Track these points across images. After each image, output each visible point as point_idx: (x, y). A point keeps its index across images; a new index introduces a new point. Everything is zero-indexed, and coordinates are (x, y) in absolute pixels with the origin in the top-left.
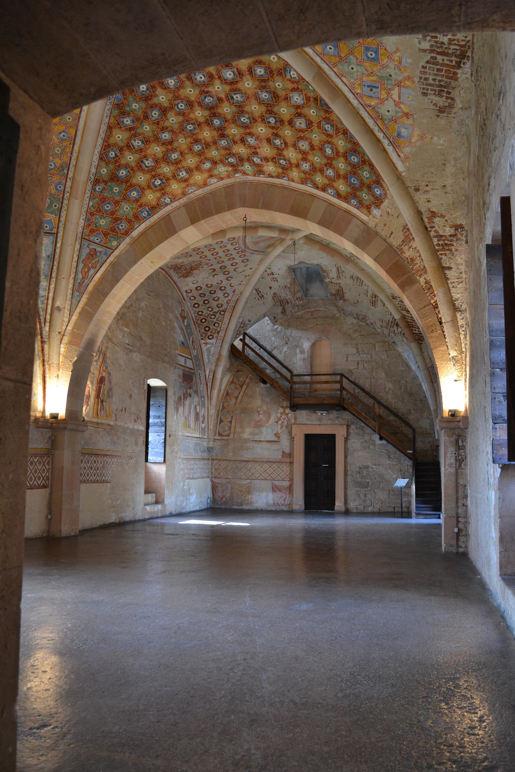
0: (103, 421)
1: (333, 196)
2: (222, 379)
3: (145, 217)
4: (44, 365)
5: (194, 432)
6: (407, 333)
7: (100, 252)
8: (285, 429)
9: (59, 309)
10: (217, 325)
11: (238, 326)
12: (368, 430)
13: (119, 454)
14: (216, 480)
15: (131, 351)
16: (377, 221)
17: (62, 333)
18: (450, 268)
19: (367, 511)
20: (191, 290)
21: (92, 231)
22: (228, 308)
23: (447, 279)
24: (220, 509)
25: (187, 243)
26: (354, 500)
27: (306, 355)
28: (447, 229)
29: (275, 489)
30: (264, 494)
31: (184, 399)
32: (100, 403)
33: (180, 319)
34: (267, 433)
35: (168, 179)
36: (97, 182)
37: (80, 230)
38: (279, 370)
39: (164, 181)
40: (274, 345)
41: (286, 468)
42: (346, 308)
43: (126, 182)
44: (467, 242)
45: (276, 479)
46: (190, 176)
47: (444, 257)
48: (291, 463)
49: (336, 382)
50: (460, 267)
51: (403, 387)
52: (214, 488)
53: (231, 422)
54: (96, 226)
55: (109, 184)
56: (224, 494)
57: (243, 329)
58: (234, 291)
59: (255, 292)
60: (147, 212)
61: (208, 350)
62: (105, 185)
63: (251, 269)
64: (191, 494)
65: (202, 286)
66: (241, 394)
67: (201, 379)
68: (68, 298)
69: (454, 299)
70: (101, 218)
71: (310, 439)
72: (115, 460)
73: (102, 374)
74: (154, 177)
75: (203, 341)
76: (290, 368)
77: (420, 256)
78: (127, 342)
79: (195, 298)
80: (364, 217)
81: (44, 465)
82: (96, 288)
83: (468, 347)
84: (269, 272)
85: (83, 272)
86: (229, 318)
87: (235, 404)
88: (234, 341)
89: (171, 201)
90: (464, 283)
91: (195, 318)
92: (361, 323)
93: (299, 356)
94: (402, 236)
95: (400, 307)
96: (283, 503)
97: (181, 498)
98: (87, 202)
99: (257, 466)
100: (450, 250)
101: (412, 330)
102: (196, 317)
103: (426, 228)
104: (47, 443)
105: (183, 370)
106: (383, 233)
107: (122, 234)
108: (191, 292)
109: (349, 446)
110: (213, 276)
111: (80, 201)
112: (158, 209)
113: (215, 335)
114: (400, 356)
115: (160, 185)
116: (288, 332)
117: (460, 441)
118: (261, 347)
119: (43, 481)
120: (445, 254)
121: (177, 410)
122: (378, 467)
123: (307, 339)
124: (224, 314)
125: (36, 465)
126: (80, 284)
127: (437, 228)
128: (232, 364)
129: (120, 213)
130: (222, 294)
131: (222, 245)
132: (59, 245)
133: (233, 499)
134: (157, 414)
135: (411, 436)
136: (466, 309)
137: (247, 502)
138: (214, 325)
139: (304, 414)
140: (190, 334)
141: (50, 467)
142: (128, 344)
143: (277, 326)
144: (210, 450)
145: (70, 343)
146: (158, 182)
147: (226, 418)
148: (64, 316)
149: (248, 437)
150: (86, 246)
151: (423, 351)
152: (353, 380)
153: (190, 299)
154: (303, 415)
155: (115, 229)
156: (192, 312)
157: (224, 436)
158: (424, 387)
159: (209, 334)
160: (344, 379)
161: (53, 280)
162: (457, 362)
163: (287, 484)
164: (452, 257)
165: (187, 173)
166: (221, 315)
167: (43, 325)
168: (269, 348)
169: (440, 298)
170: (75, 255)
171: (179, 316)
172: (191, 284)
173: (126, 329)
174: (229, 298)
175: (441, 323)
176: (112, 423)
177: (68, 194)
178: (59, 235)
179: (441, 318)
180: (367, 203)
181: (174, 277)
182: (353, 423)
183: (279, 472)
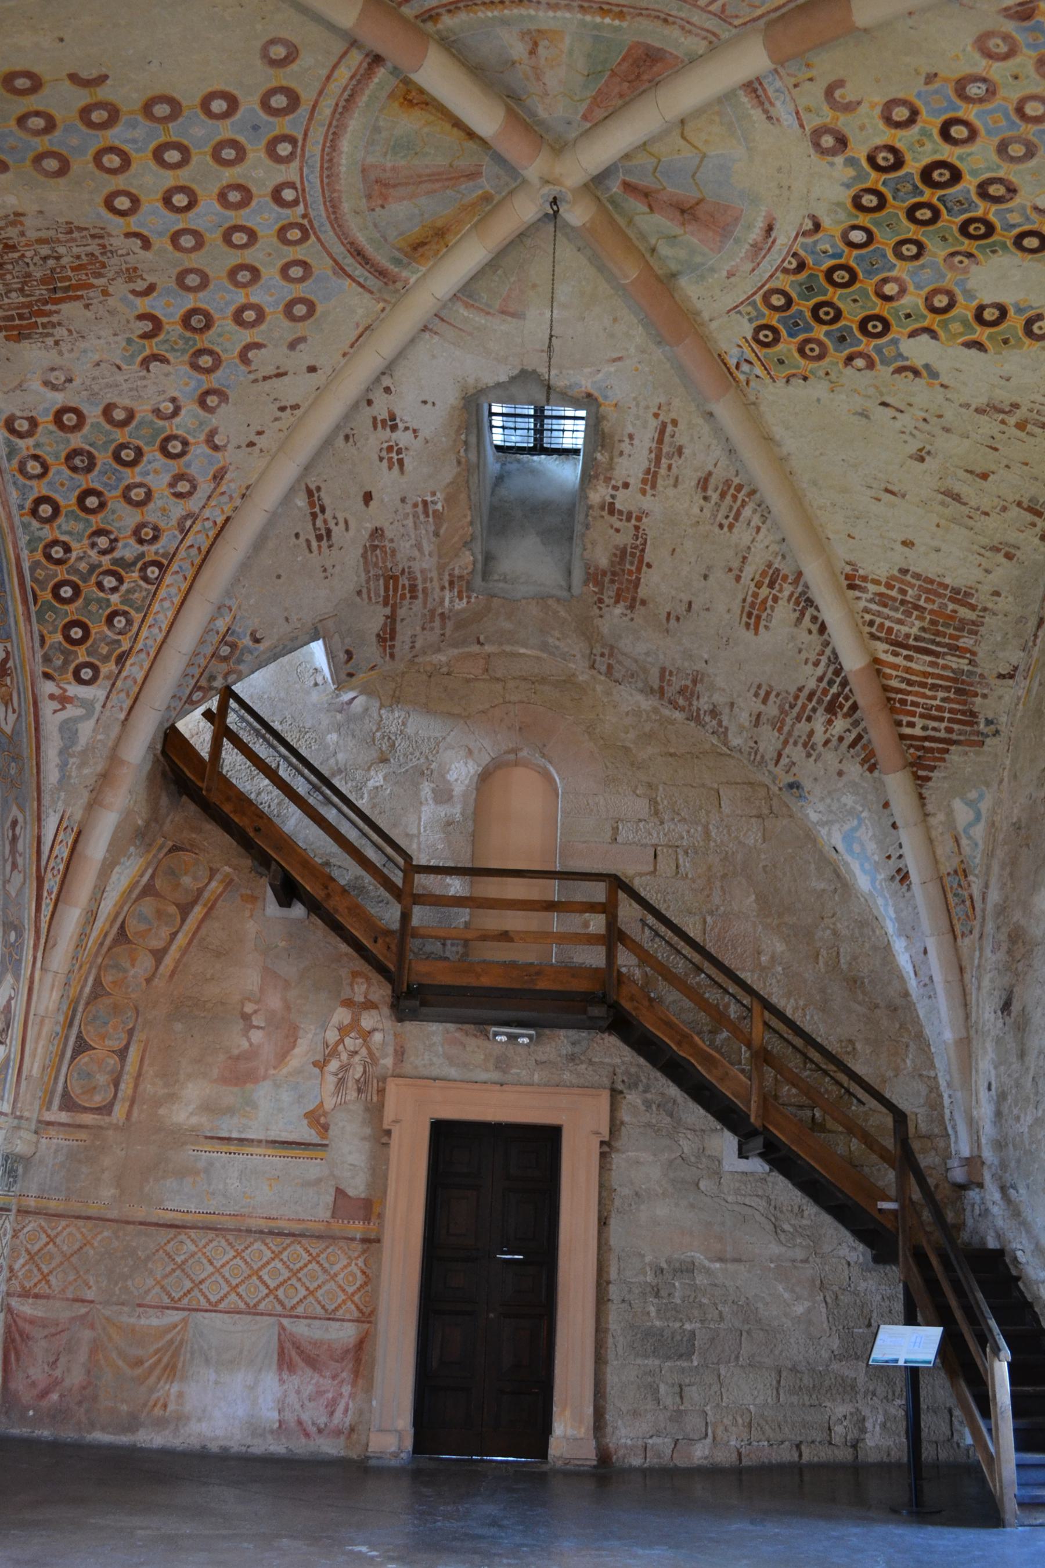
2: (108, 871)
6: (880, 734)
8: (352, 1095)
10: (120, 622)
11: (209, 650)
14: (26, 1308)
20: (33, 422)
22: (182, 553)
26: (635, 1413)
27: (456, 811)
29: (291, 1355)
30: (238, 1381)
34: (276, 1109)
40: (332, 761)
41: (344, 1265)
42: (626, 644)
45: (300, 1310)
48: (371, 1242)
49: (592, 907)
51: (823, 952)
53: (122, 1054)
56: (58, 1373)
57: (223, 667)
58: (219, 477)
61: (69, 730)
63: (312, 369)
65: (85, 409)
66: (181, 939)
67: (20, 846)
71: (454, 1145)
75: (49, 687)
84: (380, 409)
86: (177, 600)
87: (148, 981)
88: (183, 714)
91: (32, 570)
92: (666, 712)
93: (429, 812)
95: (871, 623)
96: (322, 1420)
99: (221, 1251)
101: (899, 724)
102: (35, 566)
108: (30, 433)
109: (615, 1178)
110: (146, 363)
113: (106, 669)
114: (810, 838)
116: (393, 719)
122: (731, 1267)
123: (462, 753)
124: (160, 580)
128: (155, 817)
130: (167, 478)
133: (95, 1398)
137: (158, 1411)
138: (110, 620)
139: (437, 1039)
143: (351, 695)
147: (103, 1037)
149: (194, 1120)
151: (930, 808)
153: (22, 470)
154: (433, 1042)
156: (23, 540)
157: (86, 1110)
158: (904, 961)
159: (82, 655)
163: (345, 1333)
166: (145, 579)
172: (36, 385)
174: (193, 504)
182: (636, 1085)
183: (314, 1278)
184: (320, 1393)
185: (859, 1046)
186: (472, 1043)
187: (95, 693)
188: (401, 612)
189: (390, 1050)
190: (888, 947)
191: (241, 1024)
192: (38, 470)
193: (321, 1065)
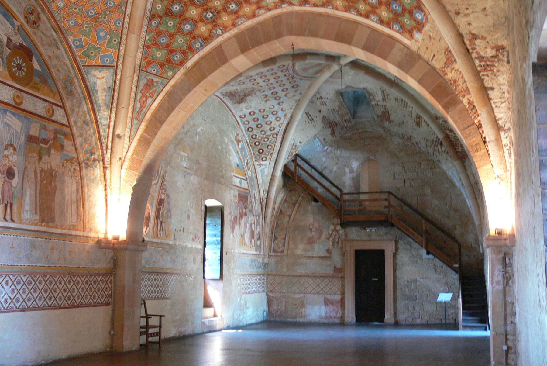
0: (163, 241)
1: (376, 22)
3: (198, 48)
4: (106, 189)
5: (250, 249)
7: (157, 82)
8: (336, 245)
9: (119, 136)
10: (270, 147)
12: (416, 245)
13: (178, 272)
14: (271, 295)
15: (188, 174)
16: (420, 45)
17: (123, 159)
18: (492, 89)
19: (415, 323)
21: (149, 63)
23: (490, 99)
24: (275, 322)
25: (238, 71)
26: (403, 313)
28: (489, 50)
29: (327, 302)
30: (316, 308)
31: (240, 218)
32: (159, 223)
33: (235, 142)
34: (319, 249)
35: (219, 12)
36: (153, 17)
37: (138, 62)
38: (329, 188)
39: (215, 13)
41: (337, 283)
43: (180, 17)
44: (508, 62)
46: (240, 9)
47: (486, 78)
48: (343, 278)
50: (503, 87)
51: (448, 203)
52: (270, 302)
53: (285, 239)
54: (153, 58)
55: (164, 18)
56: (279, 307)
58: (285, 115)
59: (305, 115)
60: (201, 43)
62: (161, 20)
64: (247, 308)
66: (294, 212)
68: (128, 126)
69: (497, 119)
70: (157, 50)
72: (174, 277)
73: (161, 196)
74: (206, 10)
75: (257, 163)
76: (340, 187)
77: (462, 77)
78: (185, 165)
79: (249, 123)
80: (406, 41)
81: (107, 283)
82: (154, 116)
83: (513, 165)
84: (318, 96)
85: (141, 101)
89: (222, 32)
90: (507, 102)
94: (444, 58)
96: (335, 315)
97: (238, 312)
98: (144, 36)
99: (310, 281)
100: (493, 71)
103: (468, 50)
104: (109, 263)
105: (239, 191)
106: (426, 56)
107: (178, 65)
110: (266, 101)
111: (137, 35)
112: (209, 41)
113: (268, 157)
114: (444, 173)
115: (211, 18)
117: (507, 259)
118: (313, 167)
119: (106, 299)
120: (487, 75)
122: (425, 280)
124: (277, 137)
125: (99, 283)
126: (139, 113)
127: (478, 48)
129: (175, 45)
130: (274, 119)
131: (273, 72)
132: (118, 77)
134: (214, 233)
135: (457, 251)
136: (509, 129)
137: (300, 315)
138: (267, 147)
140: (245, 156)
141: (113, 284)
142: (186, 168)
144: (265, 266)
145: (130, 168)
146: (209, 15)
147: (280, 236)
148: (124, 143)
149: (302, 253)
150: (143, 77)
151: (467, 168)
152: (399, 197)
153: (244, 123)
154: (354, 232)
155: (170, 60)
158: (468, 204)
159: (263, 155)
160: (391, 196)
161: (114, 110)
162: (502, 180)
164: (495, 78)
165: (236, 5)
167: (105, 152)
168: (319, 168)
169: (483, 117)
170: (133, 86)
171: (234, 140)
173: (183, 154)
174: (281, 121)
175: (485, 142)
176: (171, 243)
177: (126, 30)
178: (119, 68)
179: (485, 138)
180: (409, 28)
181: (229, 104)
183: (331, 286)
184: (334, 310)
185: (457, 226)
186: (362, 231)
187: (267, 162)
188: (335, 129)
189: (344, 234)
190: (465, 200)
191: (309, 231)
192: (247, 123)
193: (328, 239)
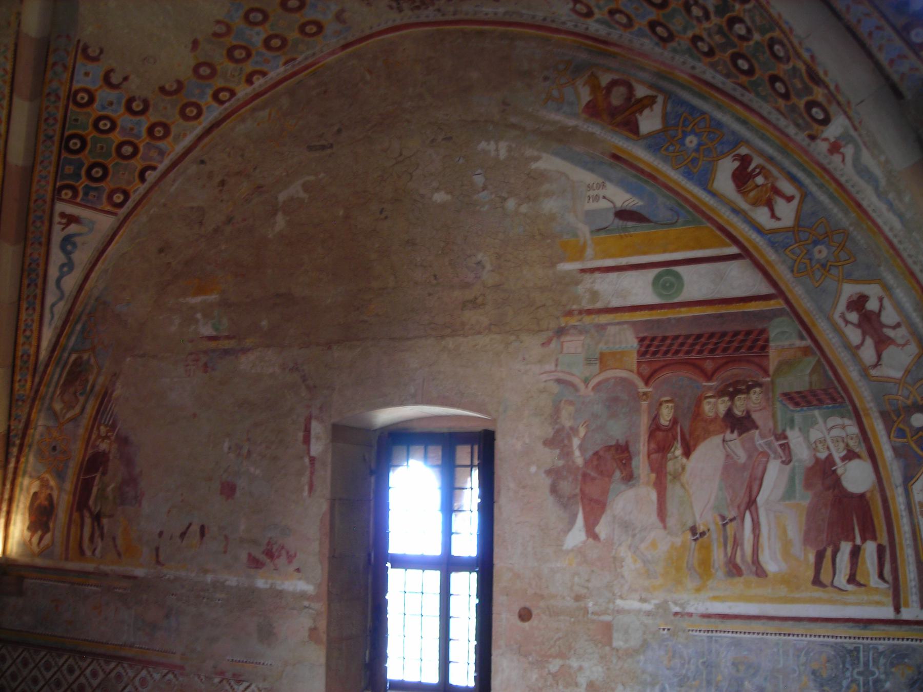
5: (818, 593)
32: (88, 521)
121: (595, 508)
176: (140, 572)
